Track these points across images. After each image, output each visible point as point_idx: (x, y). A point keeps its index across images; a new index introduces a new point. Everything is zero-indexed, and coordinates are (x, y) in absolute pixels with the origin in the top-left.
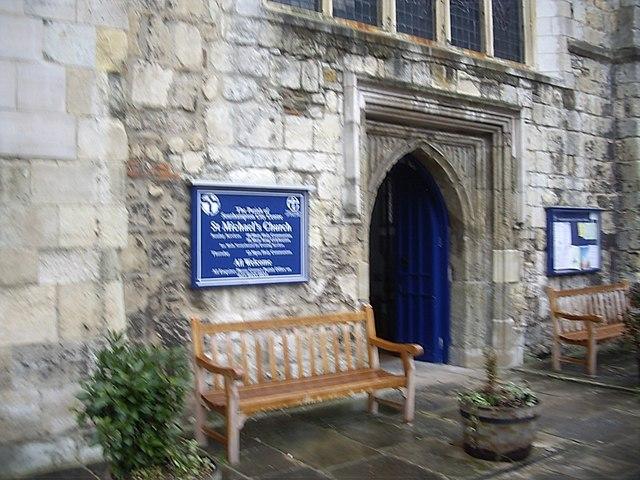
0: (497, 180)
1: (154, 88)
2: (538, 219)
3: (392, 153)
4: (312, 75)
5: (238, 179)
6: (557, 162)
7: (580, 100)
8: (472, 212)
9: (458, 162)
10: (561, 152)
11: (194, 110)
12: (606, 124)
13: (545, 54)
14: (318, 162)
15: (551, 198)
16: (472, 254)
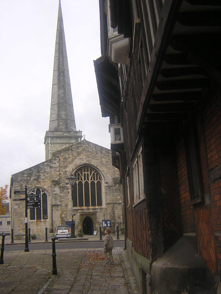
0: (96, 218)
1: (63, 215)
2: (101, 221)
3: (84, 217)
4: (75, 213)
5: (69, 221)
6: (104, 216)
7: (108, 209)
8: (94, 221)
9: (92, 217)
10: (105, 215)
11: (66, 217)
12: (113, 211)
13: (104, 205)
14: (76, 219)
15: (103, 219)
16: (94, 225)
